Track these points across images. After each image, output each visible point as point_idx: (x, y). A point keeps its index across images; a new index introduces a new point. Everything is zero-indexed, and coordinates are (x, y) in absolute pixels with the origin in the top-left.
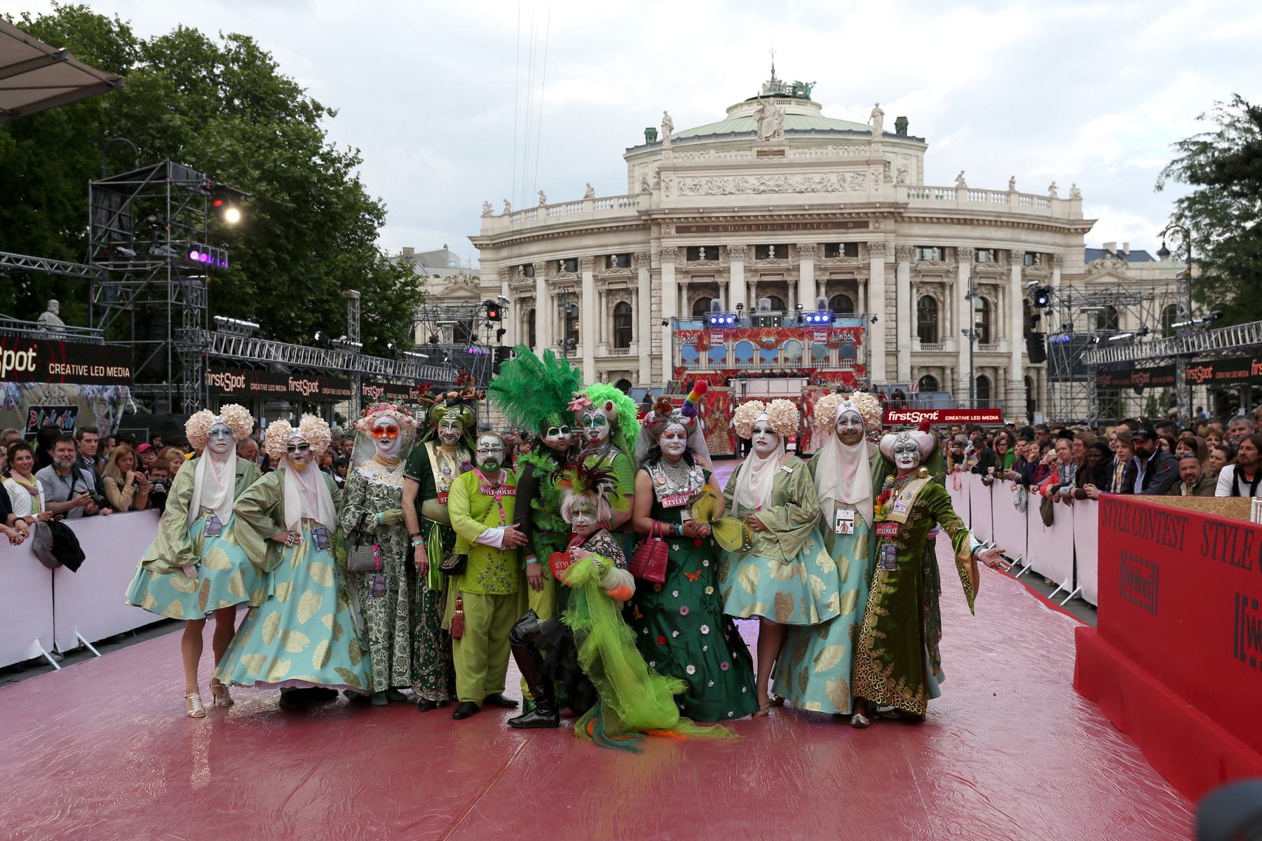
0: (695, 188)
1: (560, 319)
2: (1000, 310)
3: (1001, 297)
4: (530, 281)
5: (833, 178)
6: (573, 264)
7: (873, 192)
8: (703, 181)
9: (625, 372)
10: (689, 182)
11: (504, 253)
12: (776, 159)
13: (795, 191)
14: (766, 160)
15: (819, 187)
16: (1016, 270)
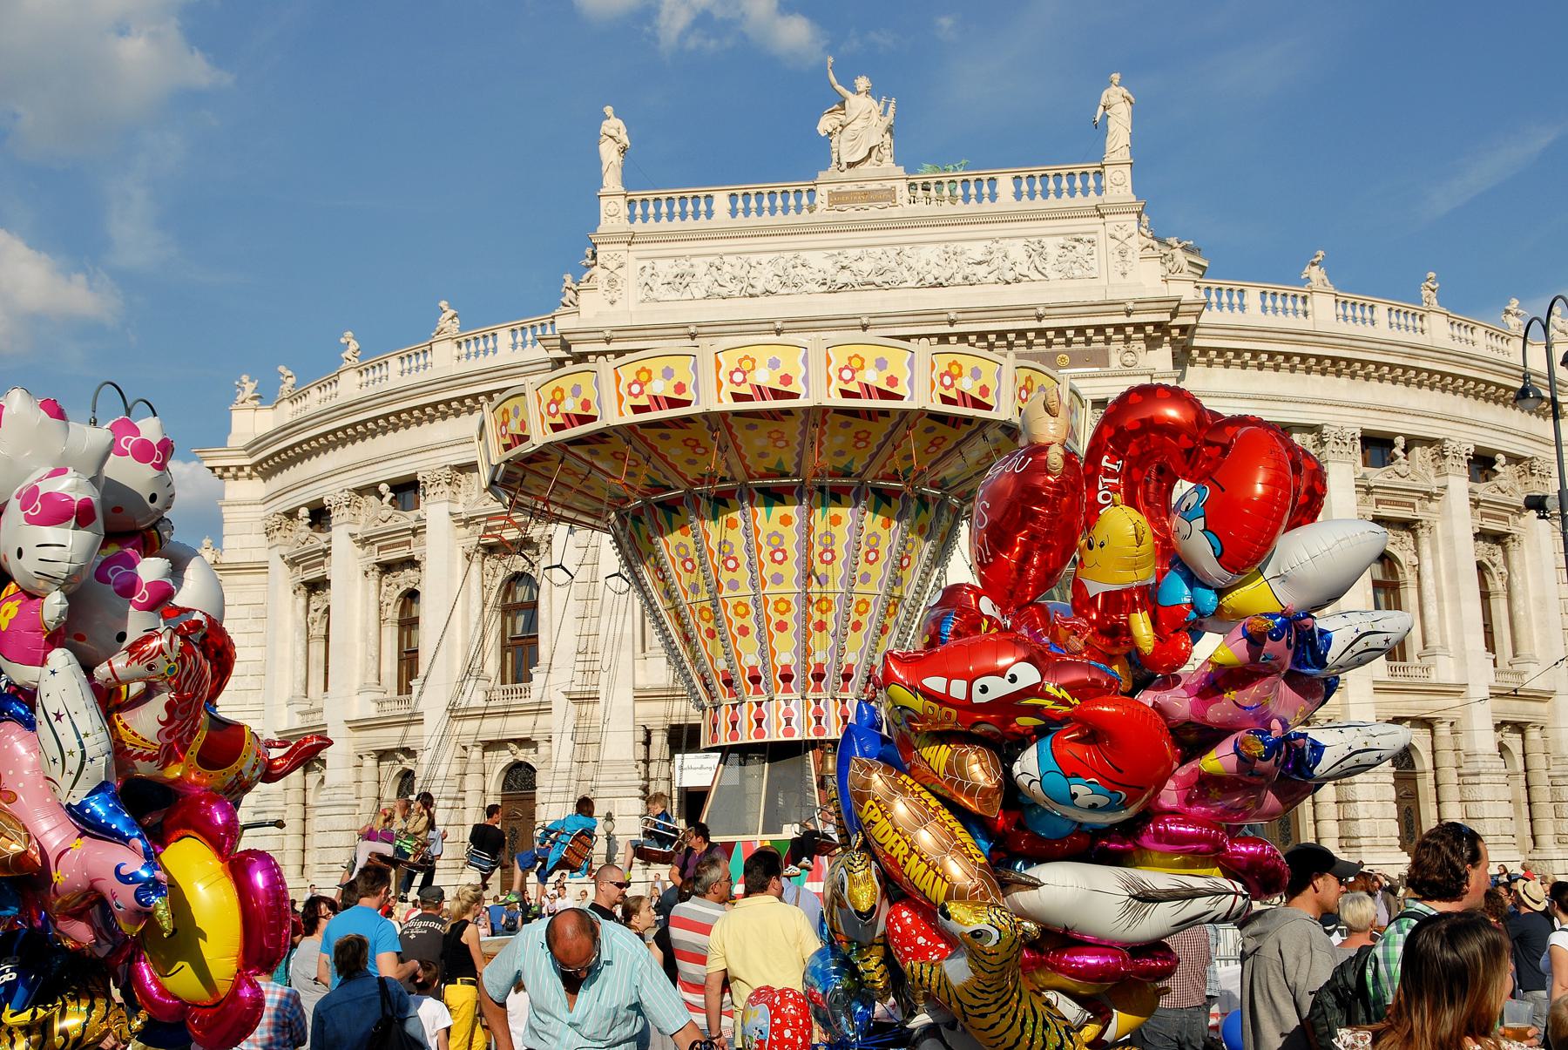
0: (681, 280)
1: (381, 621)
2: (1428, 582)
3: (1426, 549)
4: (319, 540)
5: (1017, 251)
6: (406, 490)
7: (1116, 278)
8: (701, 266)
9: (524, 743)
10: (666, 269)
11: (279, 481)
12: (874, 212)
13: (921, 284)
14: (850, 213)
15: (982, 271)
16: (1459, 484)
